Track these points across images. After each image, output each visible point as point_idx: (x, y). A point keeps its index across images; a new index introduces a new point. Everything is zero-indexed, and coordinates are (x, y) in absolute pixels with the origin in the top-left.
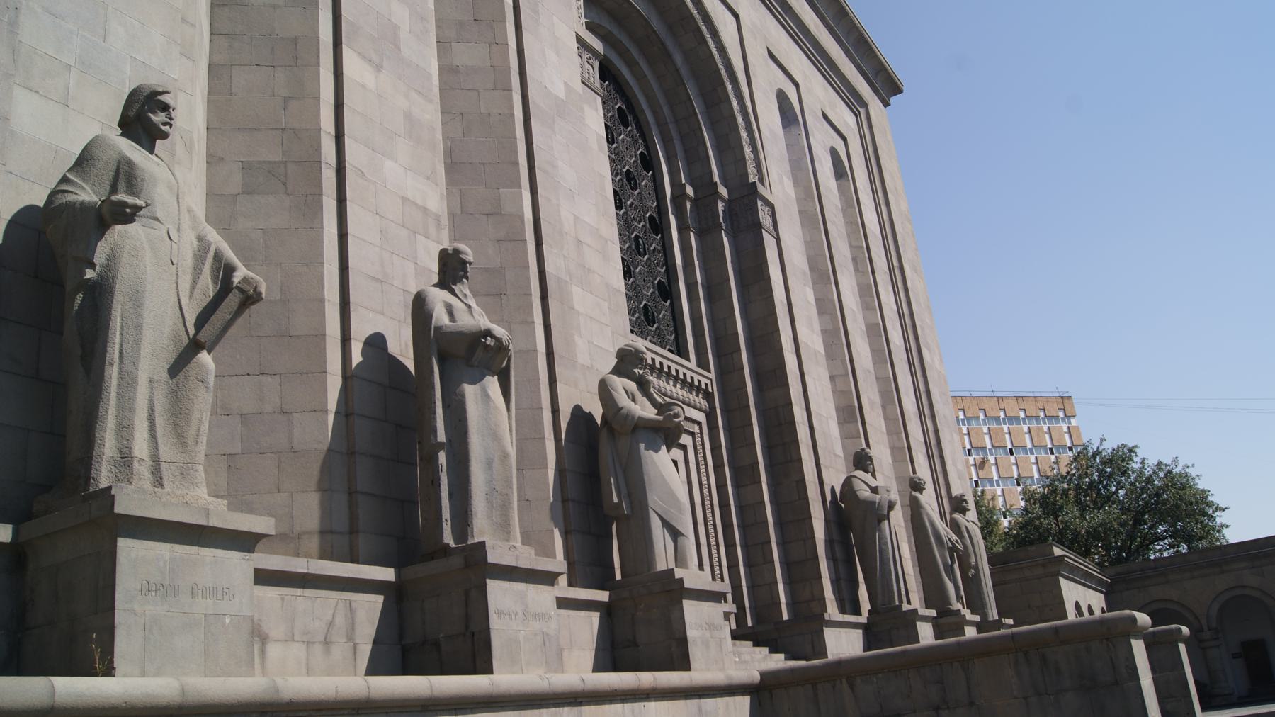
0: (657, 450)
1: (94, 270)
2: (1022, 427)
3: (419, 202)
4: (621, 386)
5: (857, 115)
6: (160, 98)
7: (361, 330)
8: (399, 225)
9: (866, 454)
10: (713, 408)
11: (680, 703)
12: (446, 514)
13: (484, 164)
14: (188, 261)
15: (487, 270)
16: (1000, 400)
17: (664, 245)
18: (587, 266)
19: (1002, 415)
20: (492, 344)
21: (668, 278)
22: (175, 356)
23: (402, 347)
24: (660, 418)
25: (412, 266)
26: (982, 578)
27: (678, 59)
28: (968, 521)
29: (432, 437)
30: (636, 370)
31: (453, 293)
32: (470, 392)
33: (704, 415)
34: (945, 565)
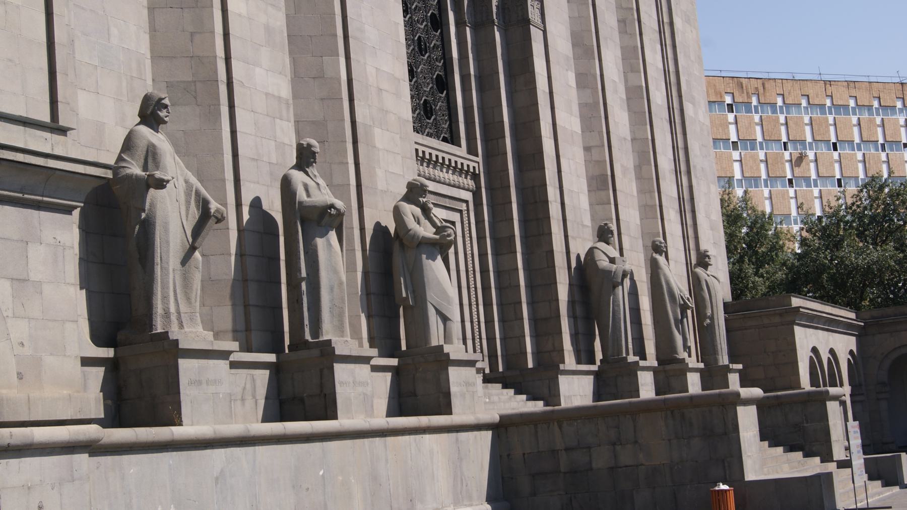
0: (434, 259)
2: (851, 118)
3: (276, 94)
4: (410, 210)
6: (163, 101)
7: (247, 200)
8: (265, 115)
9: (608, 228)
10: (478, 187)
11: (445, 436)
12: (306, 322)
13: (311, 36)
15: (313, 122)
16: (828, 86)
17: (442, 40)
18: (385, 109)
19: (828, 103)
20: (335, 213)
21: (445, 70)
22: (183, 254)
23: (274, 206)
24: (437, 237)
25: (273, 143)
26: (717, 327)
28: (708, 276)
29: (298, 274)
30: (421, 199)
31: (307, 174)
32: (320, 242)
33: (471, 194)
34: (676, 320)
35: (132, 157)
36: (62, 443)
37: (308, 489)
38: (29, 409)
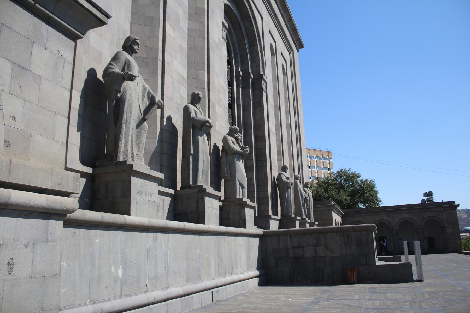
0: (239, 161)
1: (120, 94)
3: (182, 74)
5: (290, 54)
6: (137, 41)
9: (286, 167)
13: (194, 62)
14: (141, 93)
16: (309, 150)
17: (231, 91)
18: (220, 99)
20: (209, 125)
22: (138, 122)
24: (242, 151)
27: (243, 30)
30: (235, 135)
31: (196, 107)
32: (200, 138)
34: (303, 204)
35: (117, 64)
36: (40, 208)
37: (192, 260)
38: (10, 171)
